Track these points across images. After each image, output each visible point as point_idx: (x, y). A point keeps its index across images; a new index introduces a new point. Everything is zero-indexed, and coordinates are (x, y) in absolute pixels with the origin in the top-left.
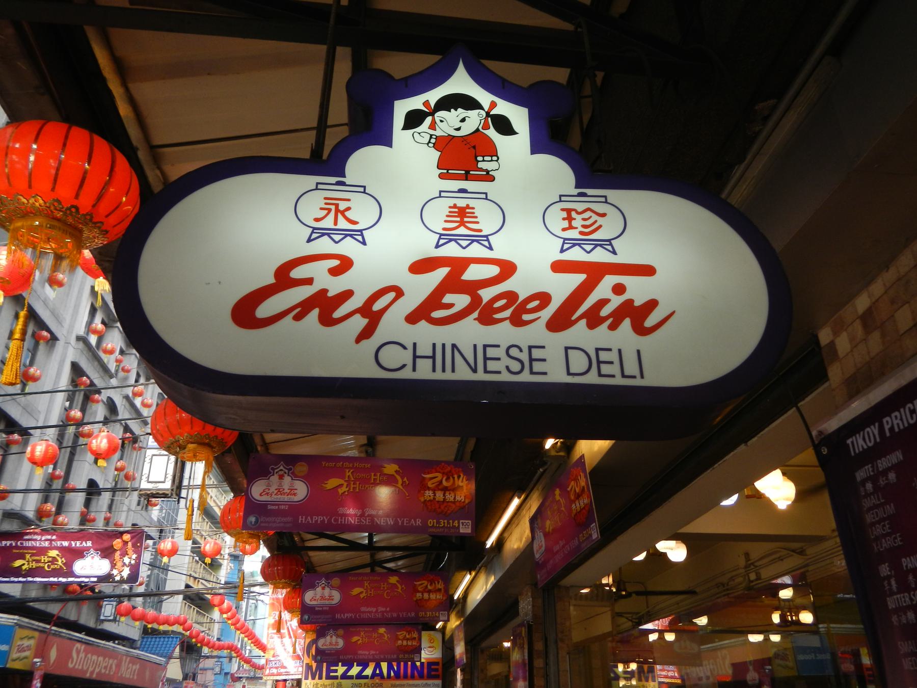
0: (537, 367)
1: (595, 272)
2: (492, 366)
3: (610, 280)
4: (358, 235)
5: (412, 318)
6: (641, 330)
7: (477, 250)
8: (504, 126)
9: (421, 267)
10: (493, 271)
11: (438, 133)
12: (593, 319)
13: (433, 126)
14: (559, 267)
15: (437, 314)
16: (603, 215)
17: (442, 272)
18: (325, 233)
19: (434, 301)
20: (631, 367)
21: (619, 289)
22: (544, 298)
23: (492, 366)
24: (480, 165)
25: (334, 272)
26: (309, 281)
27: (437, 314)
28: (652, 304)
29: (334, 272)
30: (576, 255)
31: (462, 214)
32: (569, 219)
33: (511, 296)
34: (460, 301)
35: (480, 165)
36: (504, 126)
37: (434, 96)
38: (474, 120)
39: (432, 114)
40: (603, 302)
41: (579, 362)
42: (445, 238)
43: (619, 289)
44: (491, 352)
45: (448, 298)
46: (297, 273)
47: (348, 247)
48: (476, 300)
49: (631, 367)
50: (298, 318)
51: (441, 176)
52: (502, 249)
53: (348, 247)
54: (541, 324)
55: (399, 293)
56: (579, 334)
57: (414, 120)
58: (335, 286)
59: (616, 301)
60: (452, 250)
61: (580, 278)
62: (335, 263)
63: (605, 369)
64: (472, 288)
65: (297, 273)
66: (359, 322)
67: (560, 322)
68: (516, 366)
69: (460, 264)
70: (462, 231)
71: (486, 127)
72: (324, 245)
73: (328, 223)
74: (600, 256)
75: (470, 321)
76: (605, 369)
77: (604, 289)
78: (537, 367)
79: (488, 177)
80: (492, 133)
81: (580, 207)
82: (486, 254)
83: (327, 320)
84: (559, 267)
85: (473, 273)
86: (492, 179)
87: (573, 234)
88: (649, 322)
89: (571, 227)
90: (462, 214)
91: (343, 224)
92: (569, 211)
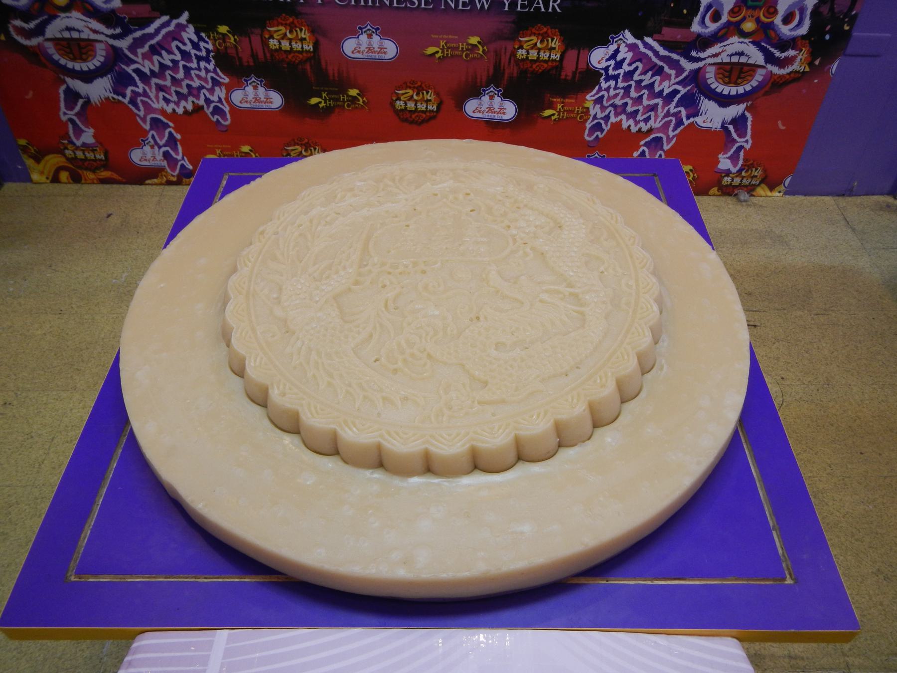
4: (482, 105)
8: (496, 94)
9: (487, 108)
12: (500, 114)
14: (499, 108)
19: (488, 111)
22: (497, 111)
31: (491, 103)
36: (496, 94)
37: (489, 91)
42: (490, 105)
52: (494, 106)
56: (499, 115)
61: (499, 110)
69: (490, 108)
83: (480, 113)
85: (492, 109)
90: (491, 103)
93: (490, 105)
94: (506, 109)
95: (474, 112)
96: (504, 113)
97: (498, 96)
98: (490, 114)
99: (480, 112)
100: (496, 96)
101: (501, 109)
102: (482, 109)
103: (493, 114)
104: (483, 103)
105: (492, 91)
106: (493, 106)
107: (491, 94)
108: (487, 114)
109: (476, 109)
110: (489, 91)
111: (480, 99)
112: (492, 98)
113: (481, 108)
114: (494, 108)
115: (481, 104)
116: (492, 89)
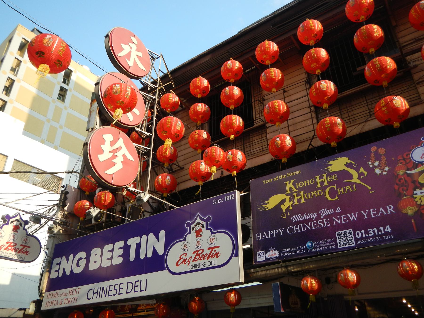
0: (205, 265)
2: (200, 266)
3: (214, 249)
4: (187, 250)
5: (193, 261)
6: (217, 257)
7: (200, 249)
9: (194, 253)
10: (201, 251)
11: (196, 230)
12: (212, 257)
13: (195, 229)
14: (209, 249)
15: (195, 260)
16: (214, 238)
17: (196, 253)
18: (184, 250)
19: (195, 258)
20: (215, 263)
22: (207, 254)
23: (200, 266)
24: (201, 234)
25: (185, 256)
26: (183, 258)
27: (195, 260)
28: (219, 252)
29: (185, 256)
30: (211, 246)
31: (198, 242)
32: (211, 240)
33: (203, 255)
34: (198, 257)
35: (201, 234)
36: (203, 226)
37: (195, 224)
38: (200, 226)
39: (195, 227)
40: (213, 253)
41: (209, 263)
42: (197, 247)
44: (200, 264)
46: (181, 257)
47: (187, 252)
48: (200, 256)
49: (215, 263)
50: (182, 264)
51: (196, 237)
53: (187, 252)
54: (206, 259)
55: (191, 257)
56: (210, 259)
58: (185, 258)
59: (215, 253)
60: (197, 249)
62: (185, 254)
63: (212, 264)
65: (181, 257)
66: (188, 263)
67: (208, 259)
68: (203, 266)
69: (198, 251)
70: (198, 246)
71: (201, 227)
72: (184, 252)
73: (184, 249)
74: (214, 246)
75: (199, 260)
76: (212, 264)
77: (213, 252)
78: (205, 265)
79: (201, 236)
80: (202, 228)
81: (212, 238)
82: (201, 249)
83: (185, 263)
84: (209, 249)
87: (211, 243)
88: (218, 256)
89: (211, 241)
90: (198, 242)
91: (186, 248)
92: (211, 239)
93: (197, 247)
94: (218, 247)
95: (177, 265)
96: (217, 255)
97: (207, 229)
98: (199, 261)
100: (204, 229)
102: (188, 257)
103: (203, 261)
105: (199, 223)
106: (200, 247)
107: (198, 227)
108: (195, 263)
109: (181, 258)
110: (195, 224)
111: (185, 240)
112: (198, 233)
113: (186, 254)
114: (203, 250)
115: (186, 249)
116: (198, 220)
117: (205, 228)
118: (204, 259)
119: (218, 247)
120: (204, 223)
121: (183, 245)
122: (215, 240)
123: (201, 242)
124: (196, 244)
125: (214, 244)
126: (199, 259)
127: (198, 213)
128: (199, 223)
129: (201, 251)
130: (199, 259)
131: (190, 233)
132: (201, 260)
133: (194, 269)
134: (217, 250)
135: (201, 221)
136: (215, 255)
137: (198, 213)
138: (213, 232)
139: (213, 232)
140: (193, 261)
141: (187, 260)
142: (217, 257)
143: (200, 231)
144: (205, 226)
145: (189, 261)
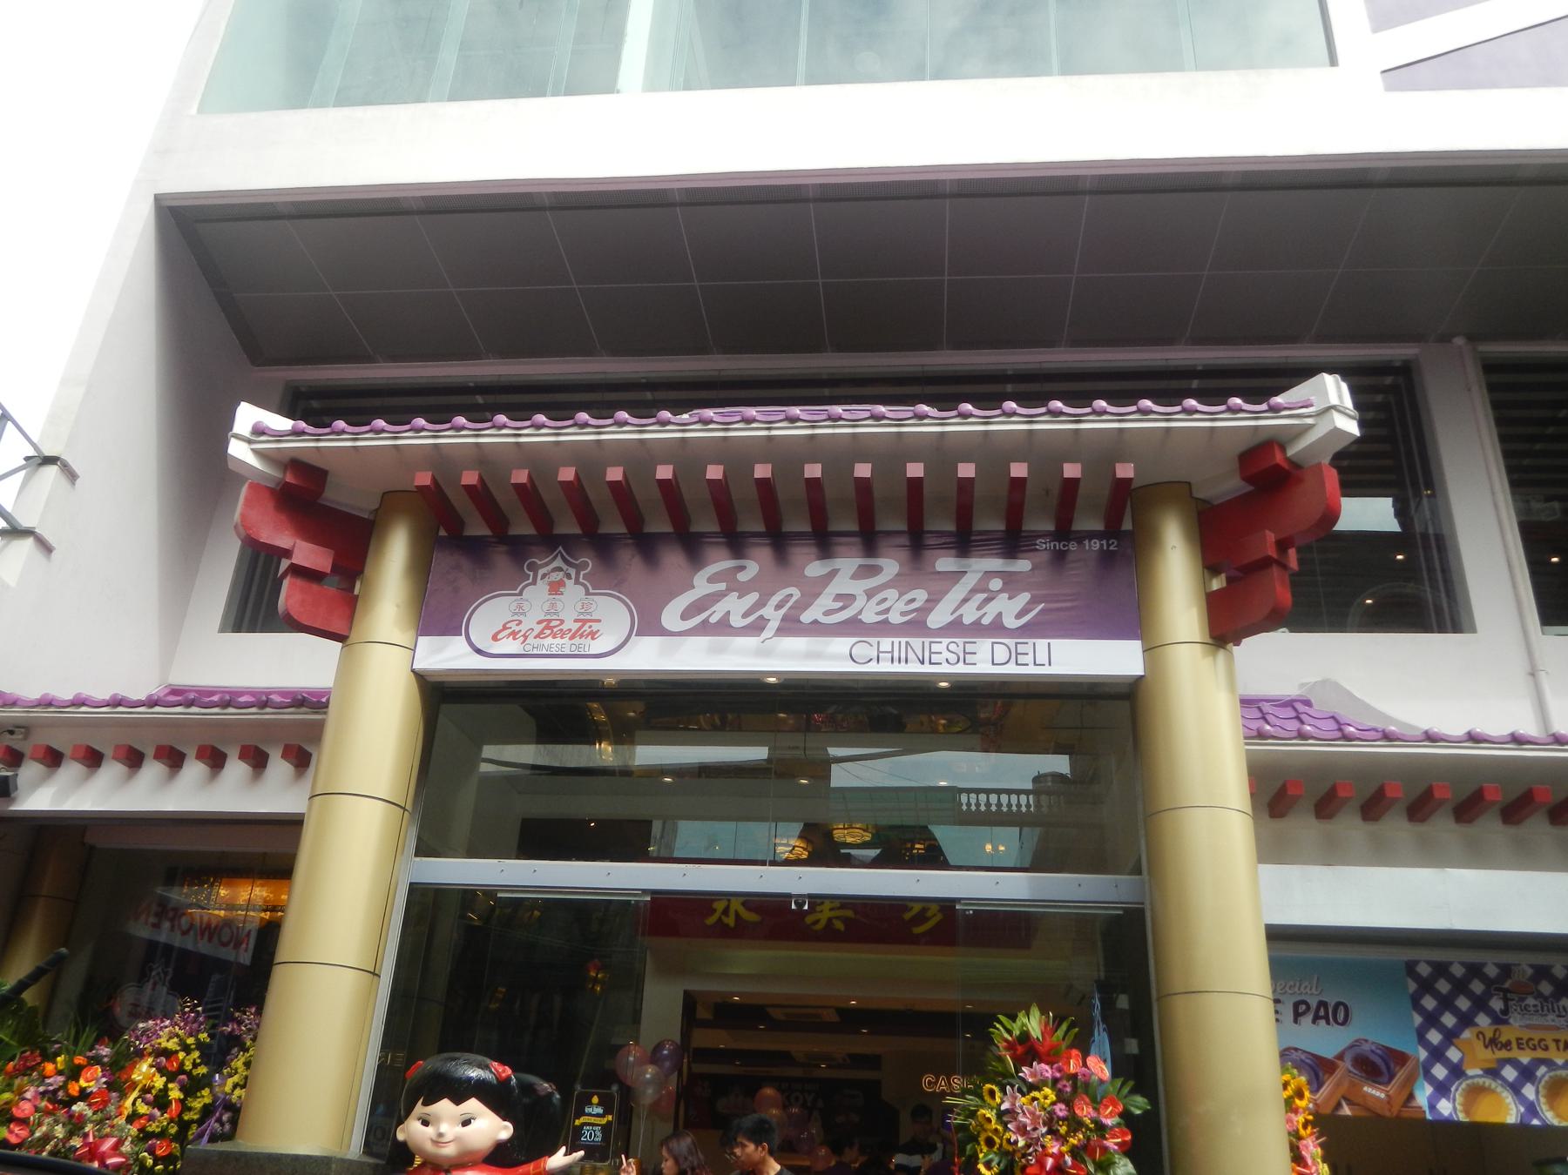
1: (584, 622)
3: (589, 624)
4: (524, 614)
8: (569, 576)
10: (558, 622)
12: (581, 636)
14: (576, 621)
17: (545, 623)
19: (542, 632)
21: (590, 627)
22: (570, 630)
30: (582, 617)
33: (561, 630)
34: (548, 632)
40: (585, 631)
41: (574, 647)
42: (548, 613)
43: (590, 627)
45: (545, 631)
47: (521, 618)
49: (587, 649)
56: (577, 640)
57: (544, 576)
58: (517, 629)
59: (589, 630)
60: (548, 617)
61: (580, 624)
64: (552, 628)
66: (522, 639)
69: (550, 621)
72: (516, 617)
74: (589, 617)
75: (550, 638)
77: (586, 628)
80: (565, 579)
83: (514, 639)
85: (552, 624)
86: (562, 594)
87: (583, 611)
93: (548, 613)
94: (599, 621)
96: (593, 635)
97: (577, 582)
98: (549, 640)
99: (514, 634)
101: (584, 622)
102: (524, 628)
103: (558, 641)
104: (526, 606)
109: (505, 628)
111: (520, 594)
114: (562, 622)
117: (573, 581)
118: (562, 637)
119: (599, 621)
120: (573, 572)
121: (515, 604)
122: (594, 606)
123: (559, 606)
124: (546, 606)
125: (590, 614)
126: (549, 635)
127: (560, 548)
128: (560, 569)
129: (558, 622)
130: (549, 635)
131: (534, 583)
132: (554, 637)
133: (535, 652)
134: (595, 626)
135: (565, 567)
136: (587, 636)
137: (560, 548)
138: (591, 591)
139: (591, 591)
140: (535, 638)
141: (522, 633)
142: (593, 639)
143: (561, 584)
144: (573, 576)
145: (526, 637)
